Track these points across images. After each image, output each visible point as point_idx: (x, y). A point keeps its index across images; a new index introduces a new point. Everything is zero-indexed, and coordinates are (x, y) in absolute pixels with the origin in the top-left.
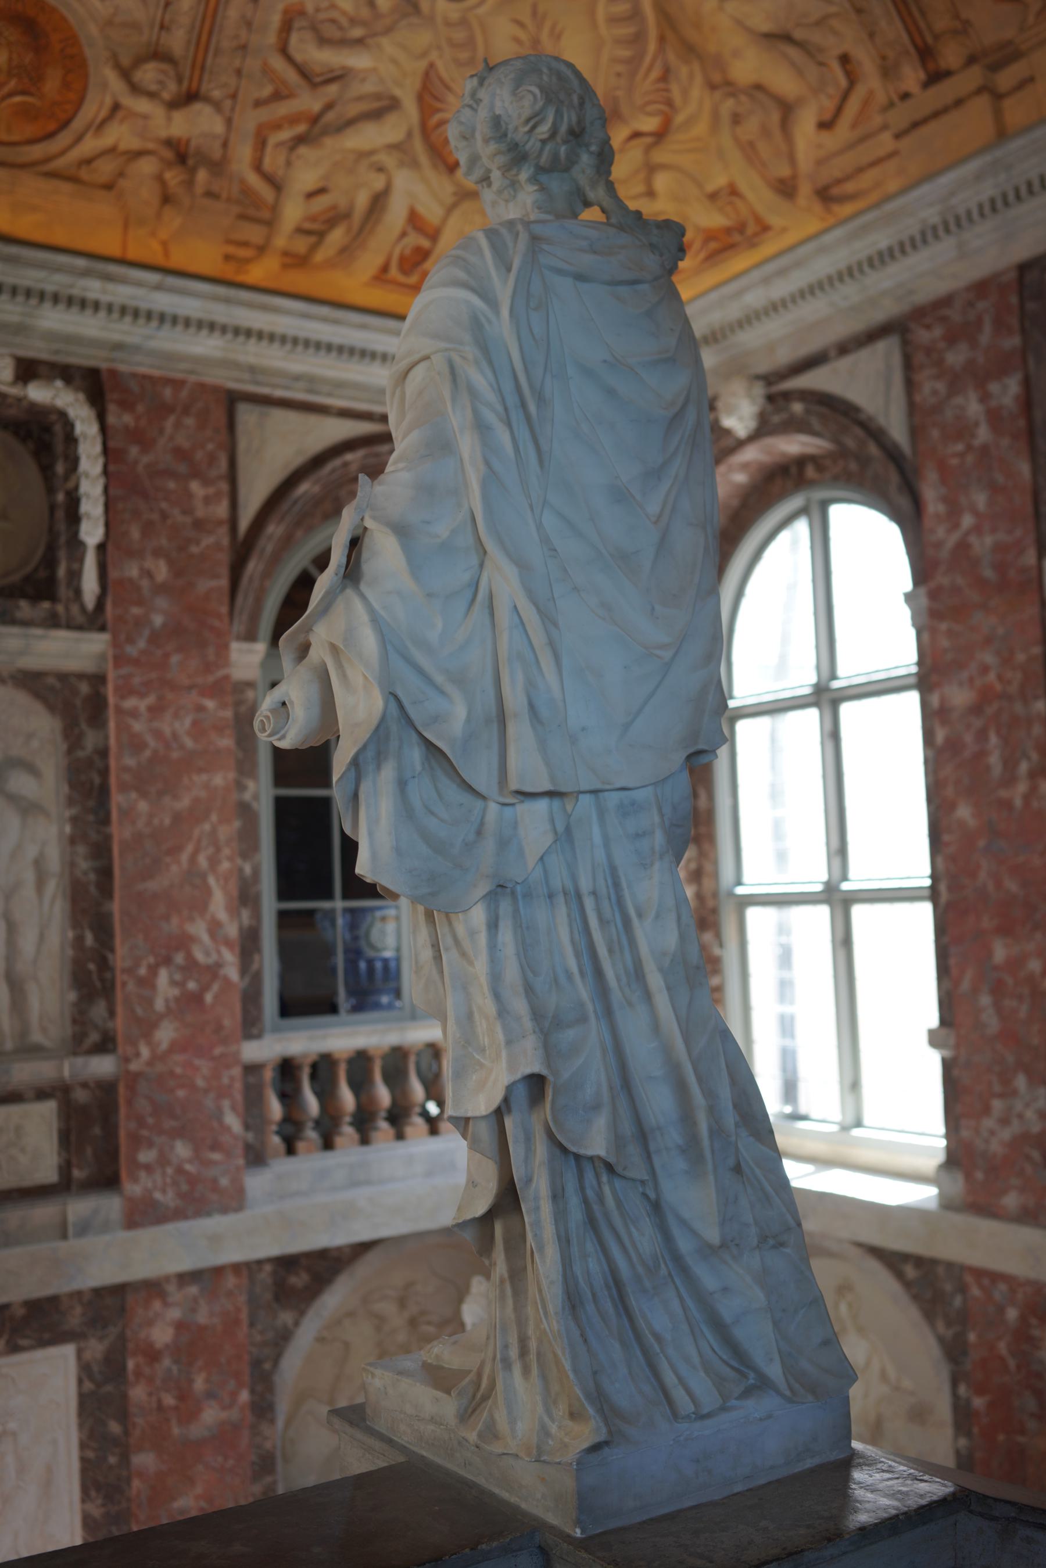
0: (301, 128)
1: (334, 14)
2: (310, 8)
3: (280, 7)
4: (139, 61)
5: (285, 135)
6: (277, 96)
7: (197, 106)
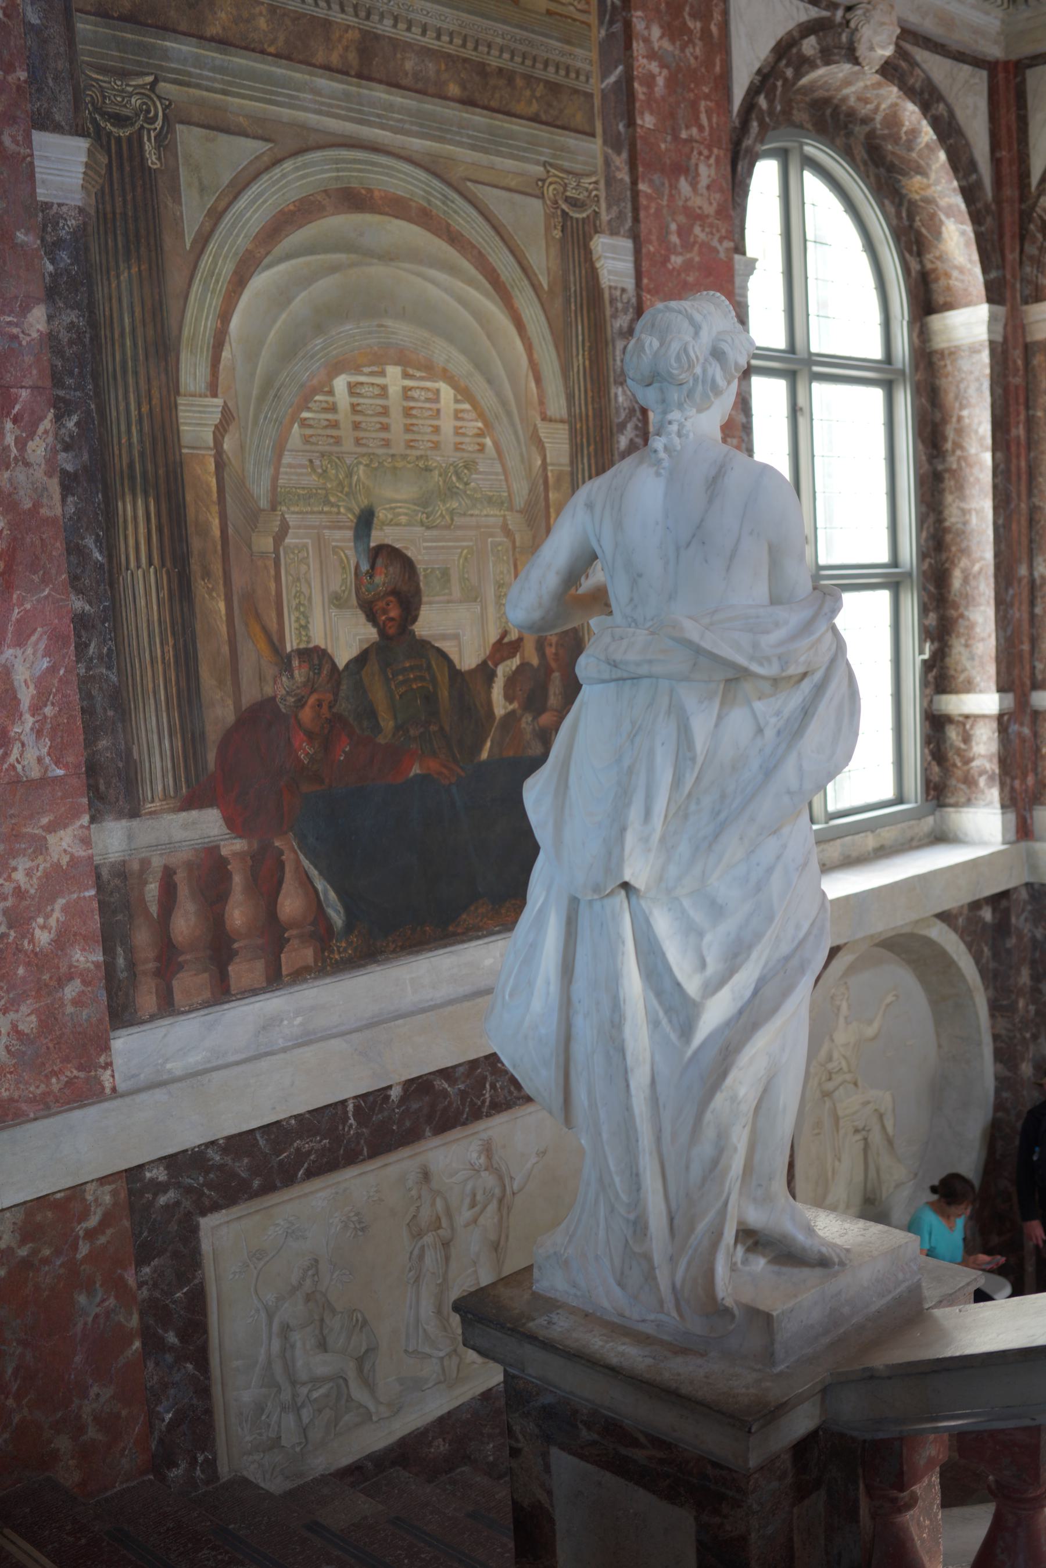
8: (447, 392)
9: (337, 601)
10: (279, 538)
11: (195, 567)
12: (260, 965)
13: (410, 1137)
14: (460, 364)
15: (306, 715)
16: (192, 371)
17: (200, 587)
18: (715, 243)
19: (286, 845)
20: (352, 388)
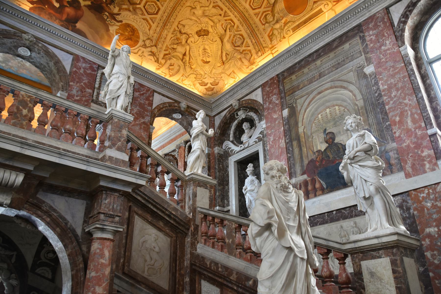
8: (337, 107)
9: (321, 143)
10: (312, 138)
11: (302, 146)
12: (313, 194)
13: (338, 220)
14: (339, 102)
15: (318, 159)
16: (300, 124)
17: (303, 148)
18: (393, 50)
19: (317, 178)
20: (321, 115)
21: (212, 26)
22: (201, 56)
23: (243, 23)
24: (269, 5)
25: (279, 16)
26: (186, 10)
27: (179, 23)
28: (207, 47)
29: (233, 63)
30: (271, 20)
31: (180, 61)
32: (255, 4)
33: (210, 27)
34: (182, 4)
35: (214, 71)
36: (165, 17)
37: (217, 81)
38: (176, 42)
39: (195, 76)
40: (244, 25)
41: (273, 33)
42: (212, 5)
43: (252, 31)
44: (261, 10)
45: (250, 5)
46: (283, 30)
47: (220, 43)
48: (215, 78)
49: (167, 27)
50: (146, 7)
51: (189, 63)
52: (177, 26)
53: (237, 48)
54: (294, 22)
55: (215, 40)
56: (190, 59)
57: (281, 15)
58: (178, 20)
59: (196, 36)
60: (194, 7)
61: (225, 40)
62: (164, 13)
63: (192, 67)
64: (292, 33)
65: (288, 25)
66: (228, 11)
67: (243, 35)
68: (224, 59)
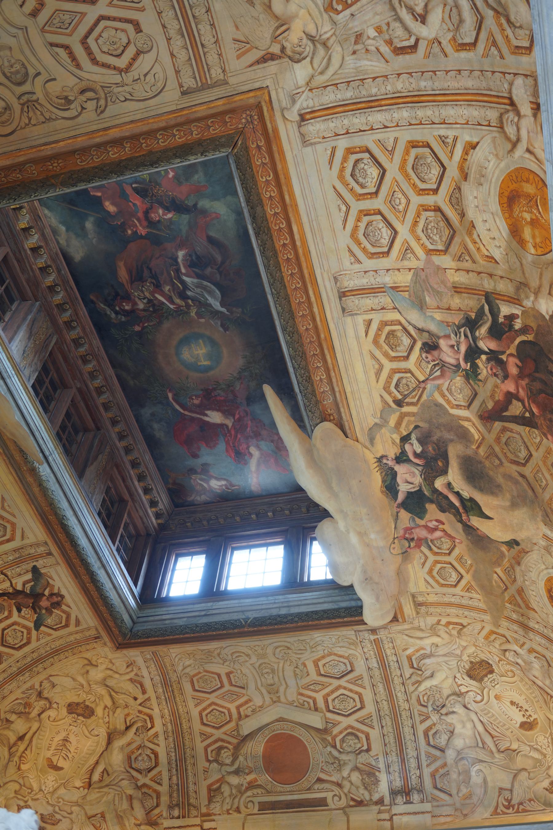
0: (503, 21)
1: (446, 16)
2: (450, 35)
3: (456, 54)
4: (508, 139)
5: (509, 32)
6: (495, 43)
7: (515, 98)
21: (106, 707)
22: (51, 752)
23: (170, 734)
24: (235, 733)
25: (246, 764)
26: (76, 663)
27: (47, 679)
28: (72, 738)
29: (110, 797)
30: (228, 761)
31: (6, 749)
32: (210, 717)
33: (103, 707)
34: (75, 651)
35: (62, 791)
36: (29, 659)
37: (58, 817)
38: (21, 709)
39: (17, 787)
40: (171, 739)
41: (220, 787)
42: (132, 675)
43: (181, 760)
44: (218, 734)
45: (200, 714)
46: (242, 794)
47: (104, 744)
48: (57, 809)
49: (21, 678)
50: (5, 632)
51: (21, 756)
52: (41, 682)
53: (135, 774)
54: (268, 792)
55: (96, 733)
56: (26, 749)
57: (250, 765)
58: (49, 671)
59: (64, 711)
60: (94, 663)
61: (118, 743)
62: (33, 652)
63: (22, 766)
64: (256, 811)
65: (255, 791)
66: (154, 701)
67: (160, 755)
68: (96, 777)
